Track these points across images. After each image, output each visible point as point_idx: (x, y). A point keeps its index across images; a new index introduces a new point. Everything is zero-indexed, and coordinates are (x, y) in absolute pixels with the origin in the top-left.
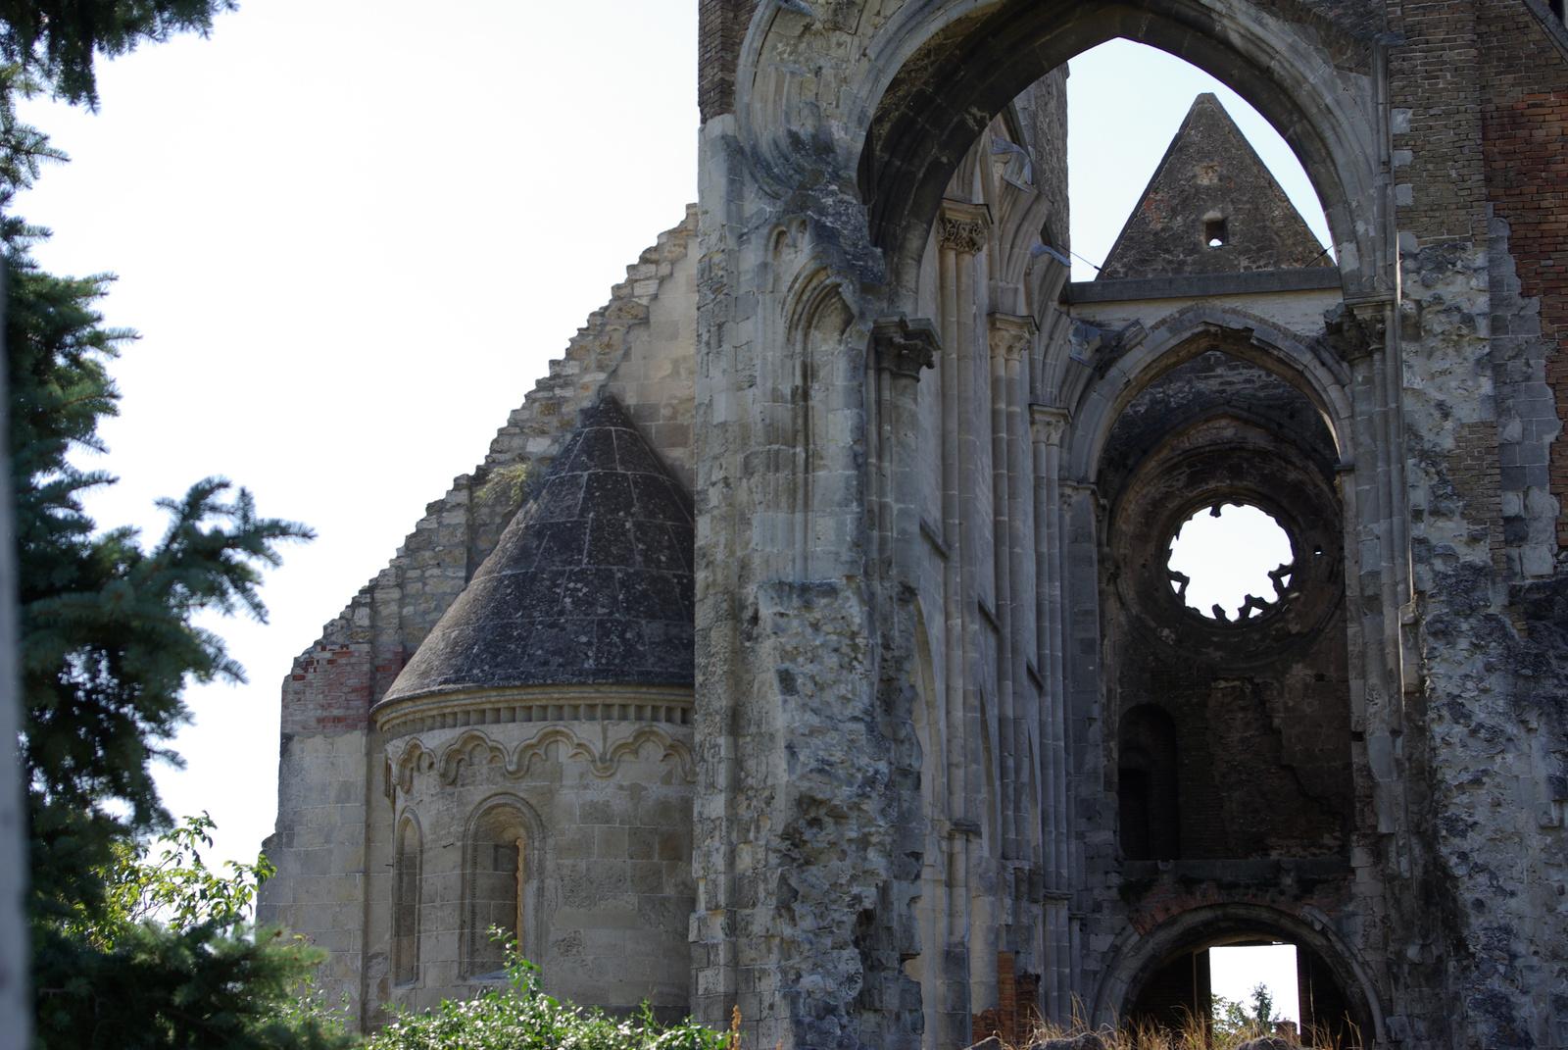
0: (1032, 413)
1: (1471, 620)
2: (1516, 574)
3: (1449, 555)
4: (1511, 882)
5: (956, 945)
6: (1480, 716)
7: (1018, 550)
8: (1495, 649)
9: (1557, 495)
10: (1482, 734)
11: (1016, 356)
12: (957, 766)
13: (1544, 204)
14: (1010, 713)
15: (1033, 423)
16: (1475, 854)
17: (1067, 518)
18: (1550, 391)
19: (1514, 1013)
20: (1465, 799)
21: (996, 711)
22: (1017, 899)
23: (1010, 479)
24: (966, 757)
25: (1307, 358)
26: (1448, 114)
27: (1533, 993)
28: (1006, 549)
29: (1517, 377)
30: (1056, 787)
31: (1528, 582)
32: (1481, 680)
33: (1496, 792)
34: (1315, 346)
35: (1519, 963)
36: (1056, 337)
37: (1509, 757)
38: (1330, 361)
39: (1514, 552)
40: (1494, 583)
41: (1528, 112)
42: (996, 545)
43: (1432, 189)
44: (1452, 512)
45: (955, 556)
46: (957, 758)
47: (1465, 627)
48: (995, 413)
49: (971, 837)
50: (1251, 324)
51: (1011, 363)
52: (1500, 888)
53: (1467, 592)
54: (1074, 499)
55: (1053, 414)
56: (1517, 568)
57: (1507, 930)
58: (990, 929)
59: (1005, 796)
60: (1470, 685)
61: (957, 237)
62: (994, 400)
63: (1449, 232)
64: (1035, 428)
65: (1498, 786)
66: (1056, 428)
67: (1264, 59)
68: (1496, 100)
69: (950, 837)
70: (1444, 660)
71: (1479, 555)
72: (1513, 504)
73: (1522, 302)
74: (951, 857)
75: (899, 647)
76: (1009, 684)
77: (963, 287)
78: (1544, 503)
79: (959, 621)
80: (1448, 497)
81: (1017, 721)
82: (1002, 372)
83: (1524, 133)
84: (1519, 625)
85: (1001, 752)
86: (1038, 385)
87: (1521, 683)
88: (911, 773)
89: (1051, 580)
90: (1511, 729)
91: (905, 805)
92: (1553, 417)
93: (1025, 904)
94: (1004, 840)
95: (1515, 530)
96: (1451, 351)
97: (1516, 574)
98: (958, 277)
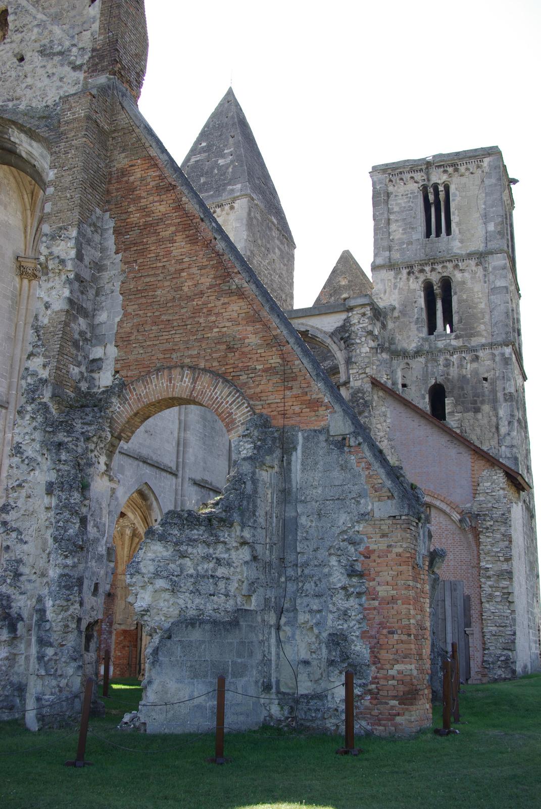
1: (33, 405)
2: (95, 386)
3: (35, 374)
4: (27, 536)
6: (30, 452)
8: (40, 419)
9: (117, 346)
10: (26, 462)
13: (130, 210)
16: (13, 523)
18: (121, 297)
19: (13, 604)
20: (15, 495)
25: (329, 341)
26: (70, 169)
27: (28, 594)
29: (108, 292)
31: (101, 390)
32: (32, 434)
33: (30, 491)
34: (332, 335)
35: (22, 578)
37: (37, 472)
38: (336, 341)
39: (96, 375)
40: (47, 386)
41: (129, 169)
43: (59, 204)
44: (39, 354)
47: (29, 408)
50: (308, 328)
52: (21, 540)
53: (33, 392)
56: (97, 383)
57: (20, 561)
60: (27, 437)
61: (27, 273)
63: (63, 222)
65: (30, 488)
67: (33, 161)
68: (117, 166)
70: (20, 426)
71: (44, 374)
72: (97, 352)
73: (115, 256)
77: (31, 294)
78: (112, 351)
80: (38, 346)
83: (125, 179)
84: (55, 407)
87: (47, 435)
90: (39, 459)
92: (119, 309)
95: (95, 365)
96: (57, 278)
97: (95, 386)
98: (29, 290)
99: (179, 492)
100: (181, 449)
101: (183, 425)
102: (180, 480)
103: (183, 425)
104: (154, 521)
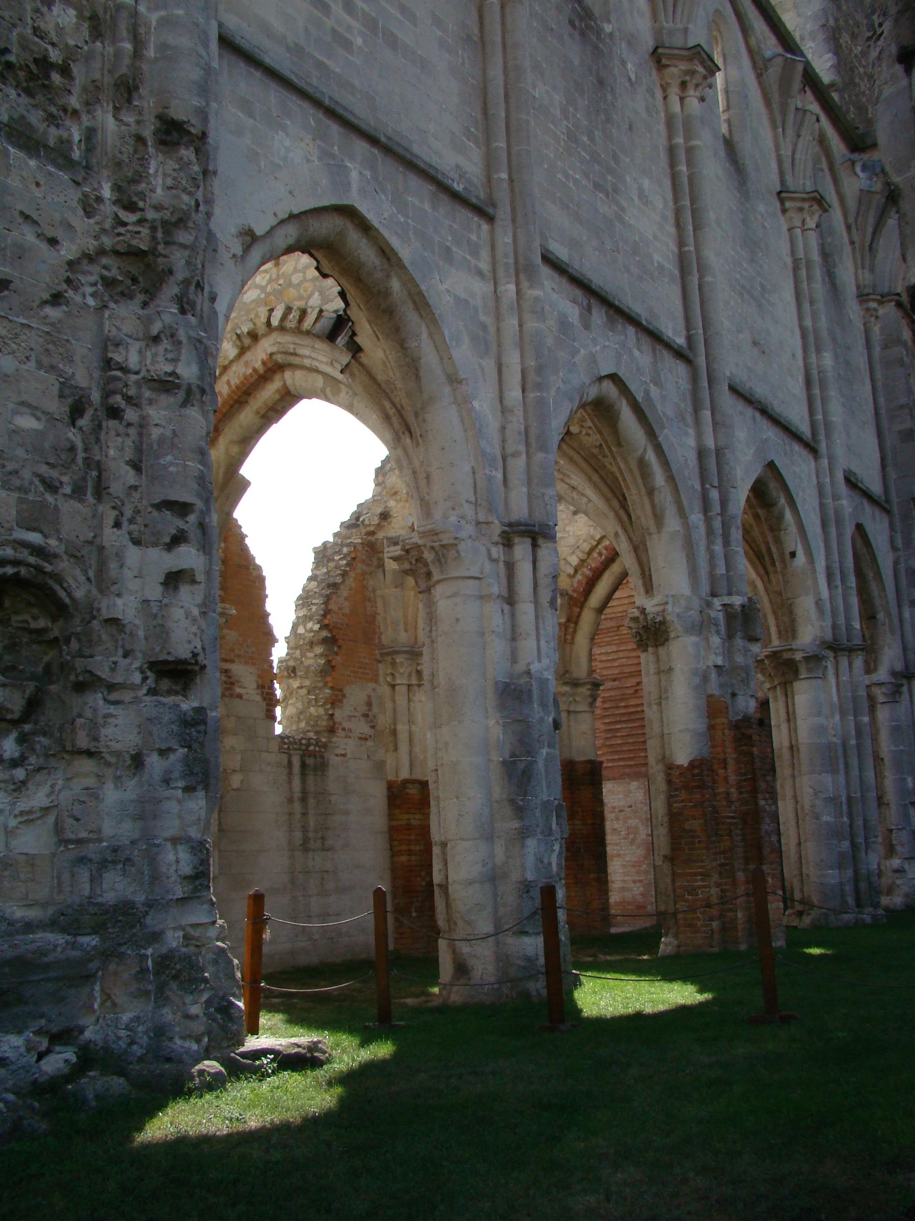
0: (782, 201)
5: (520, 676)
7: (708, 279)
11: (691, 92)
12: (515, 455)
14: (710, 443)
15: (784, 211)
17: (876, 329)
21: (691, 442)
22: (730, 636)
23: (694, 212)
24: (528, 445)
28: (695, 279)
30: (840, 543)
36: (803, 132)
42: (683, 277)
45: (503, 213)
46: (515, 445)
48: (672, 151)
49: (540, 541)
51: (687, 100)
54: (881, 312)
55: (803, 200)
58: (695, 672)
59: (710, 532)
62: (670, 137)
64: (787, 214)
66: (812, 214)
69: (507, 542)
74: (510, 567)
75: (158, 208)
76: (707, 414)
79: (512, 287)
81: (719, 452)
82: (676, 108)
85: (703, 485)
86: (789, 178)
88: (178, 386)
89: (818, 351)
91: (155, 433)
93: (739, 642)
94: (712, 576)
99: (828, 489)
100: (817, 391)
101: (811, 339)
102: (825, 462)
103: (811, 339)
104: (788, 557)
